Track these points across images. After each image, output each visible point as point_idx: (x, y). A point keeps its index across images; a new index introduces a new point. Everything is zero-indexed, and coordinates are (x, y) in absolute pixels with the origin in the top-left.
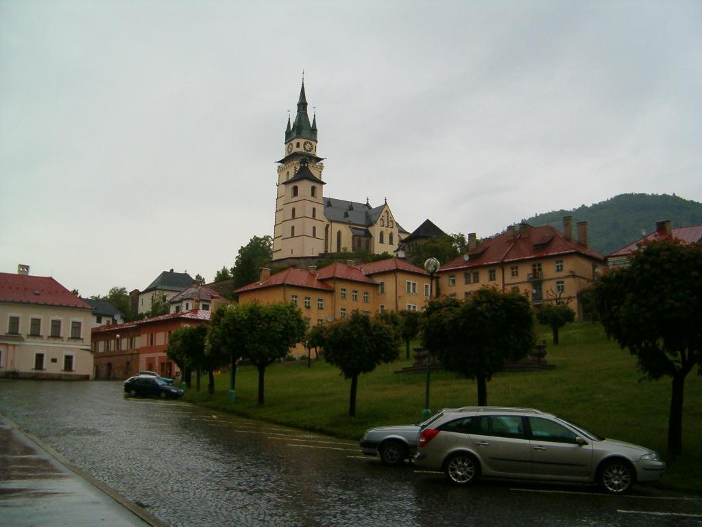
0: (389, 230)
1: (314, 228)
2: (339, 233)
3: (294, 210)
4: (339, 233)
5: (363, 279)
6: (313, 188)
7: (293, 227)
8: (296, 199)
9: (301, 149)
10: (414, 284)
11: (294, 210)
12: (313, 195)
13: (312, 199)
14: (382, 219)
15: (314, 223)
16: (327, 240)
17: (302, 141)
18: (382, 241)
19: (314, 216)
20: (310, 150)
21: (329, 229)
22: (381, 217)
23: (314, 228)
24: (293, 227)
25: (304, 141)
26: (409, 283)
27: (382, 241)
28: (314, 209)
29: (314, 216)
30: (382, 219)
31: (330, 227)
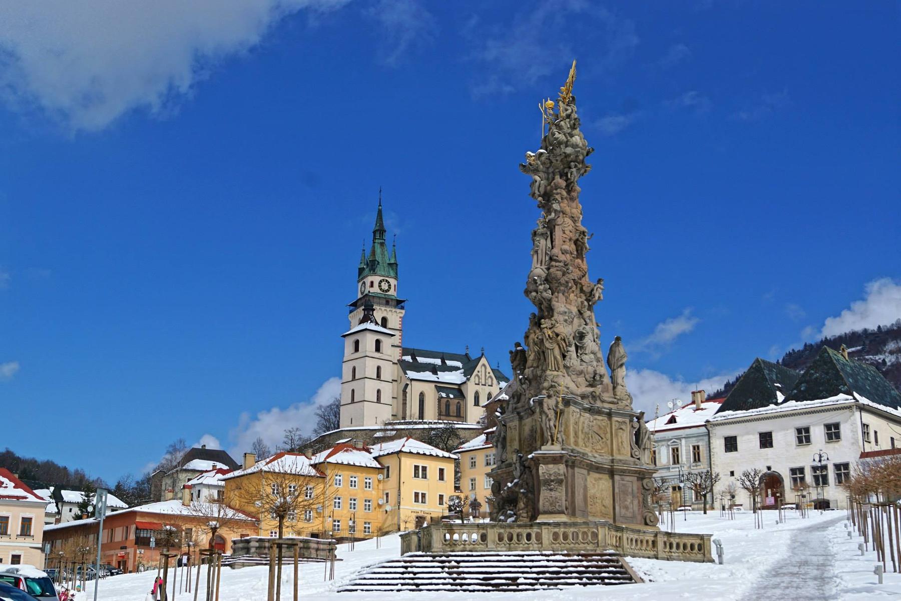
0: (487, 389)
1: (379, 391)
2: (422, 395)
3: (354, 369)
4: (422, 395)
5: (375, 464)
6: (378, 342)
7: (353, 391)
8: (357, 355)
9: (376, 289)
10: (424, 469)
11: (354, 369)
12: (378, 349)
13: (377, 355)
14: (477, 375)
15: (378, 385)
16: (405, 404)
17: (376, 279)
18: (477, 403)
19: (378, 376)
20: (388, 291)
21: (408, 390)
22: (475, 372)
23: (379, 391)
24: (353, 391)
25: (379, 279)
26: (416, 467)
27: (477, 403)
28: (379, 368)
29: (378, 376)
30: (477, 375)
31: (409, 386)
